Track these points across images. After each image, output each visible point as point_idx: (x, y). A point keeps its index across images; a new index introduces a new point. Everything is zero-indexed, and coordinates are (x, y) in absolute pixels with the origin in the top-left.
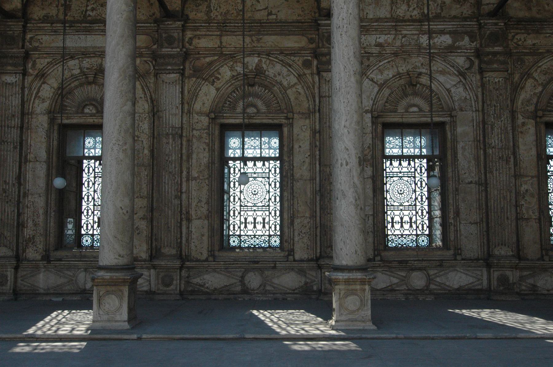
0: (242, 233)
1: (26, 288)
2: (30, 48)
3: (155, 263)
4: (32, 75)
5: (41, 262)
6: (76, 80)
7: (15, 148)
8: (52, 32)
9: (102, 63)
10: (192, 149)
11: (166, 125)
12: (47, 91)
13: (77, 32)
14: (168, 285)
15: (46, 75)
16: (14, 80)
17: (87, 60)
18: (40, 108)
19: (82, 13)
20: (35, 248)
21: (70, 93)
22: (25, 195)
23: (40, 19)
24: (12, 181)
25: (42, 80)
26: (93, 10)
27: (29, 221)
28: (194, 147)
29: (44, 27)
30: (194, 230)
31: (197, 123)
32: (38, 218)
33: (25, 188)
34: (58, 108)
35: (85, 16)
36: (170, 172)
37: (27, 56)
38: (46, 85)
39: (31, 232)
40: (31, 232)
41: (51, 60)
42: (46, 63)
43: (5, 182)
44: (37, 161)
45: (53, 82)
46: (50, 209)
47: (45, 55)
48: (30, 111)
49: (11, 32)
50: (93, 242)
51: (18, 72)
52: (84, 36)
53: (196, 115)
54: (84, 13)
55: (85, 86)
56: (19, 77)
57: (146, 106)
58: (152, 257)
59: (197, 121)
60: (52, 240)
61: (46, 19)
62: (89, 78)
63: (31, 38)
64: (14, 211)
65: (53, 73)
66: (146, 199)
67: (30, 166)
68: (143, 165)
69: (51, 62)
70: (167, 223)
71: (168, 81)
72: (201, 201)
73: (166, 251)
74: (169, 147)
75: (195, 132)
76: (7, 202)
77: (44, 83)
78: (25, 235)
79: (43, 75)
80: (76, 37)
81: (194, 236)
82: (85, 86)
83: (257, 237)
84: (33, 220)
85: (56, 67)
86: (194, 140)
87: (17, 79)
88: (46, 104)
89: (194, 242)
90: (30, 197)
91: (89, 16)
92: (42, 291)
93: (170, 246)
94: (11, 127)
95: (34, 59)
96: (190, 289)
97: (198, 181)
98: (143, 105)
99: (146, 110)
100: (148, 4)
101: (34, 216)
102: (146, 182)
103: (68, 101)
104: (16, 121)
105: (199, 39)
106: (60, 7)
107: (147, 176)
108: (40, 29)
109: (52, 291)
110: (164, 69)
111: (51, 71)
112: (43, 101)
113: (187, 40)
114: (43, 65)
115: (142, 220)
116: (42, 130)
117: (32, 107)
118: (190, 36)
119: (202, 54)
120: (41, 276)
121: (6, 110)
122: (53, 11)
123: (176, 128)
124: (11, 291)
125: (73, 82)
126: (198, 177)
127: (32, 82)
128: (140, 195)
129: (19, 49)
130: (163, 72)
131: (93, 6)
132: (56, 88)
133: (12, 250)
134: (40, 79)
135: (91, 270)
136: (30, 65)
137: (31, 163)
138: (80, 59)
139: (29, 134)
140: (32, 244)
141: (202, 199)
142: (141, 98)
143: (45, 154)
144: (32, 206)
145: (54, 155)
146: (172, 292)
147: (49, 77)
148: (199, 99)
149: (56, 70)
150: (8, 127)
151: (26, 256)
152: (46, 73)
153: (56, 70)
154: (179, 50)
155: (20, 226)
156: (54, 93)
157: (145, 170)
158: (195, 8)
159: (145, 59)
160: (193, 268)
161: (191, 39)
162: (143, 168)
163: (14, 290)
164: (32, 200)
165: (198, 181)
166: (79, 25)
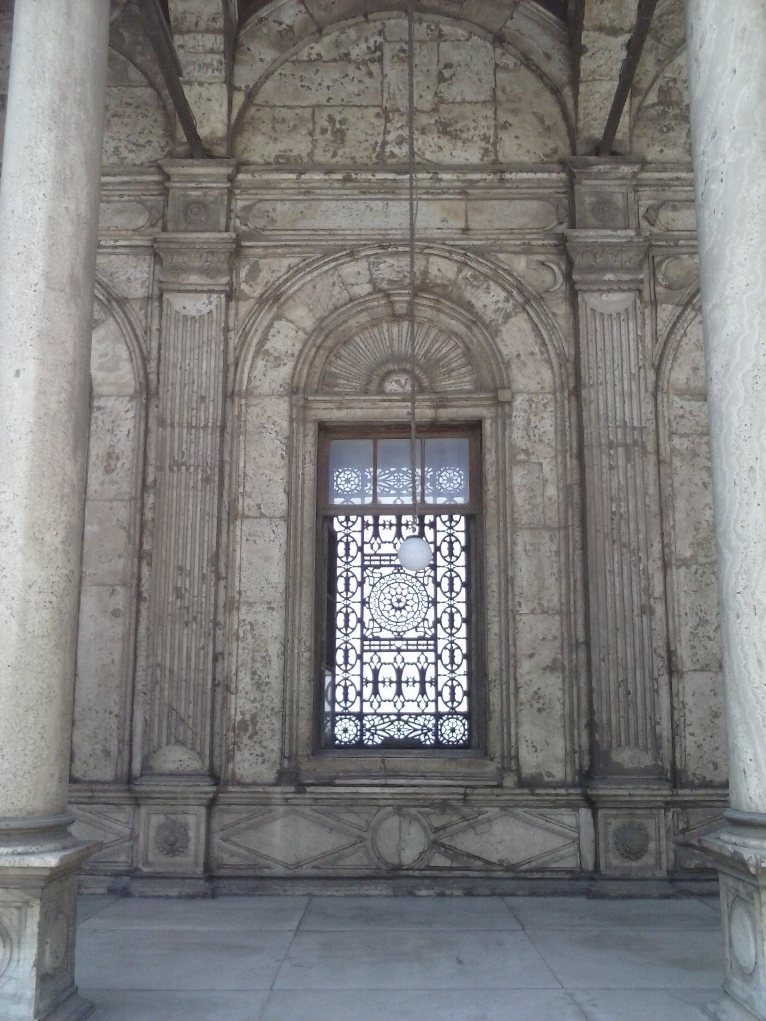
1: (235, 861)
2: (245, 232)
3: (601, 792)
4: (247, 298)
5: (278, 789)
6: (362, 310)
7: (207, 480)
8: (299, 194)
9: (427, 268)
10: (672, 485)
11: (607, 419)
12: (285, 339)
13: (364, 193)
14: (636, 854)
15: (283, 298)
16: (205, 311)
17: (390, 261)
18: (269, 378)
19: (374, 149)
20: (258, 750)
21: (345, 343)
22: (231, 606)
23: (268, 164)
24: (201, 568)
25: (275, 309)
26: (400, 142)
27: (241, 675)
28: (677, 480)
29: (279, 182)
30: (689, 700)
31: (682, 417)
32: (265, 666)
33: (233, 587)
34: (316, 379)
35: (380, 156)
36: (623, 545)
37: (237, 251)
38: (283, 322)
39: (248, 706)
40: (248, 706)
41: (297, 260)
42: (284, 270)
43: (181, 569)
44: (262, 515)
45: (302, 315)
46: (299, 642)
47: (280, 251)
48: (244, 387)
49: (198, 193)
50: (362, 735)
51: (217, 288)
52: (380, 204)
53: (676, 398)
54: (378, 149)
55: (385, 326)
56: (218, 300)
57: (547, 375)
58: (586, 777)
59: (681, 412)
60: (304, 727)
61: (283, 163)
62: (397, 306)
63: (248, 209)
64: (203, 648)
65: (302, 296)
66: (557, 617)
67: (242, 529)
68: (546, 527)
69: (297, 265)
70: (625, 681)
71: (606, 311)
72: (706, 622)
73: (625, 757)
74: (611, 475)
75: (676, 441)
76: (187, 624)
77: (278, 317)
78: (233, 712)
79: (277, 299)
80: (362, 205)
81: (691, 718)
82: (385, 326)
83: (405, 718)
84: (254, 673)
85: (309, 278)
86: (677, 462)
87: (212, 307)
88: (285, 371)
89: (692, 734)
90: (244, 609)
91: (392, 155)
92: (279, 871)
93: (637, 744)
94: (197, 428)
95: (252, 260)
96: (693, 863)
97: (694, 568)
98: (538, 373)
99: (547, 385)
100: (540, 129)
101: (254, 660)
102: (555, 570)
103: (339, 362)
104: (211, 412)
105: (674, 208)
106: (317, 136)
107: (558, 553)
108: (268, 186)
109: (306, 871)
110: (594, 282)
111: (296, 287)
112: (278, 361)
113: (642, 211)
114: (279, 274)
115: (548, 673)
116: (274, 435)
117: (249, 377)
118: (650, 202)
119: (682, 246)
120: (278, 826)
121: (183, 386)
122: (299, 145)
123: (634, 428)
124: (200, 870)
125: (354, 316)
126: (694, 557)
127: (253, 314)
128: (540, 605)
129: (220, 231)
130: (592, 287)
131: (400, 132)
132: (309, 329)
133: (200, 754)
134: (271, 307)
135: (414, 811)
136: (243, 274)
137: (246, 522)
138: (372, 259)
139: (242, 445)
140: (250, 738)
141: (708, 617)
142: (532, 354)
143: (282, 497)
144: (249, 636)
145: (306, 501)
146: (648, 874)
147: (291, 302)
148: (681, 359)
149: (309, 286)
150: (190, 426)
151: (234, 773)
152: (284, 292)
153: (309, 286)
154: (632, 233)
155: (222, 687)
156: (305, 343)
157: (552, 540)
158: (657, 135)
159: (542, 258)
160: (695, 804)
161: (657, 209)
162: (547, 535)
163: (207, 867)
164: (249, 618)
165: (694, 568)
166: (370, 177)
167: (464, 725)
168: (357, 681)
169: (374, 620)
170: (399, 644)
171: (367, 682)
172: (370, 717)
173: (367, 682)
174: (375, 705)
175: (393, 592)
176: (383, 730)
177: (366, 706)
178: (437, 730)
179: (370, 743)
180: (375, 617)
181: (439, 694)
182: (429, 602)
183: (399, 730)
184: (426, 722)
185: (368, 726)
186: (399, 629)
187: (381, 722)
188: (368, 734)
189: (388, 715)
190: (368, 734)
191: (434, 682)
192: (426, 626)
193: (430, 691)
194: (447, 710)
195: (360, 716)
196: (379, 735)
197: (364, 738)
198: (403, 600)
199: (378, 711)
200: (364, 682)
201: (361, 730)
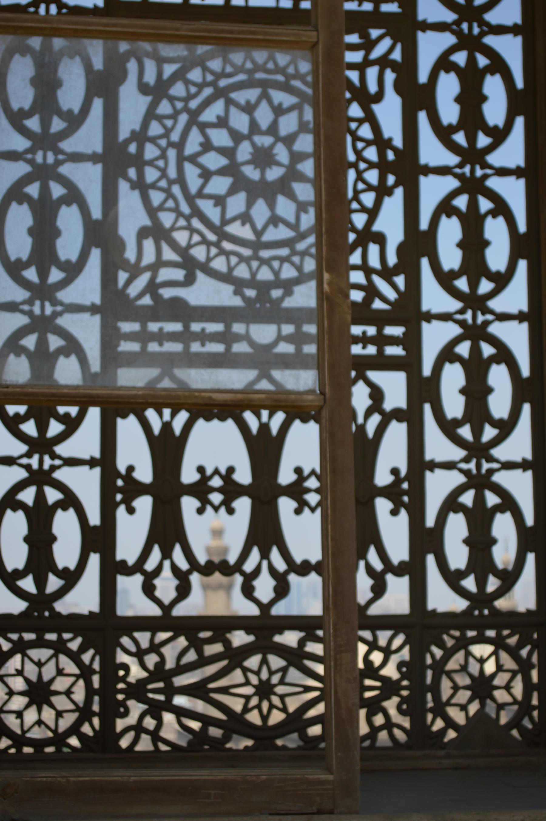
0: (132, 599)
167: (524, 667)
168: (86, 485)
169: (156, 232)
170: (263, 333)
171: (134, 489)
172: (144, 638)
173: (134, 489)
174: (166, 585)
175: (240, 121)
176: (197, 690)
177: (129, 587)
178: (419, 689)
179: (145, 744)
180: (167, 219)
181: (426, 541)
182: (383, 166)
183: (264, 690)
184: (377, 657)
185: (136, 673)
186: (265, 274)
187: (191, 656)
188: (136, 708)
189: (222, 626)
190: (136, 708)
191: (408, 493)
192: (374, 261)
193: (394, 532)
194: (460, 604)
195: (105, 628)
196: (181, 713)
197: (120, 724)
198: (282, 154)
199: (181, 610)
200: (118, 488)
201: (107, 691)
